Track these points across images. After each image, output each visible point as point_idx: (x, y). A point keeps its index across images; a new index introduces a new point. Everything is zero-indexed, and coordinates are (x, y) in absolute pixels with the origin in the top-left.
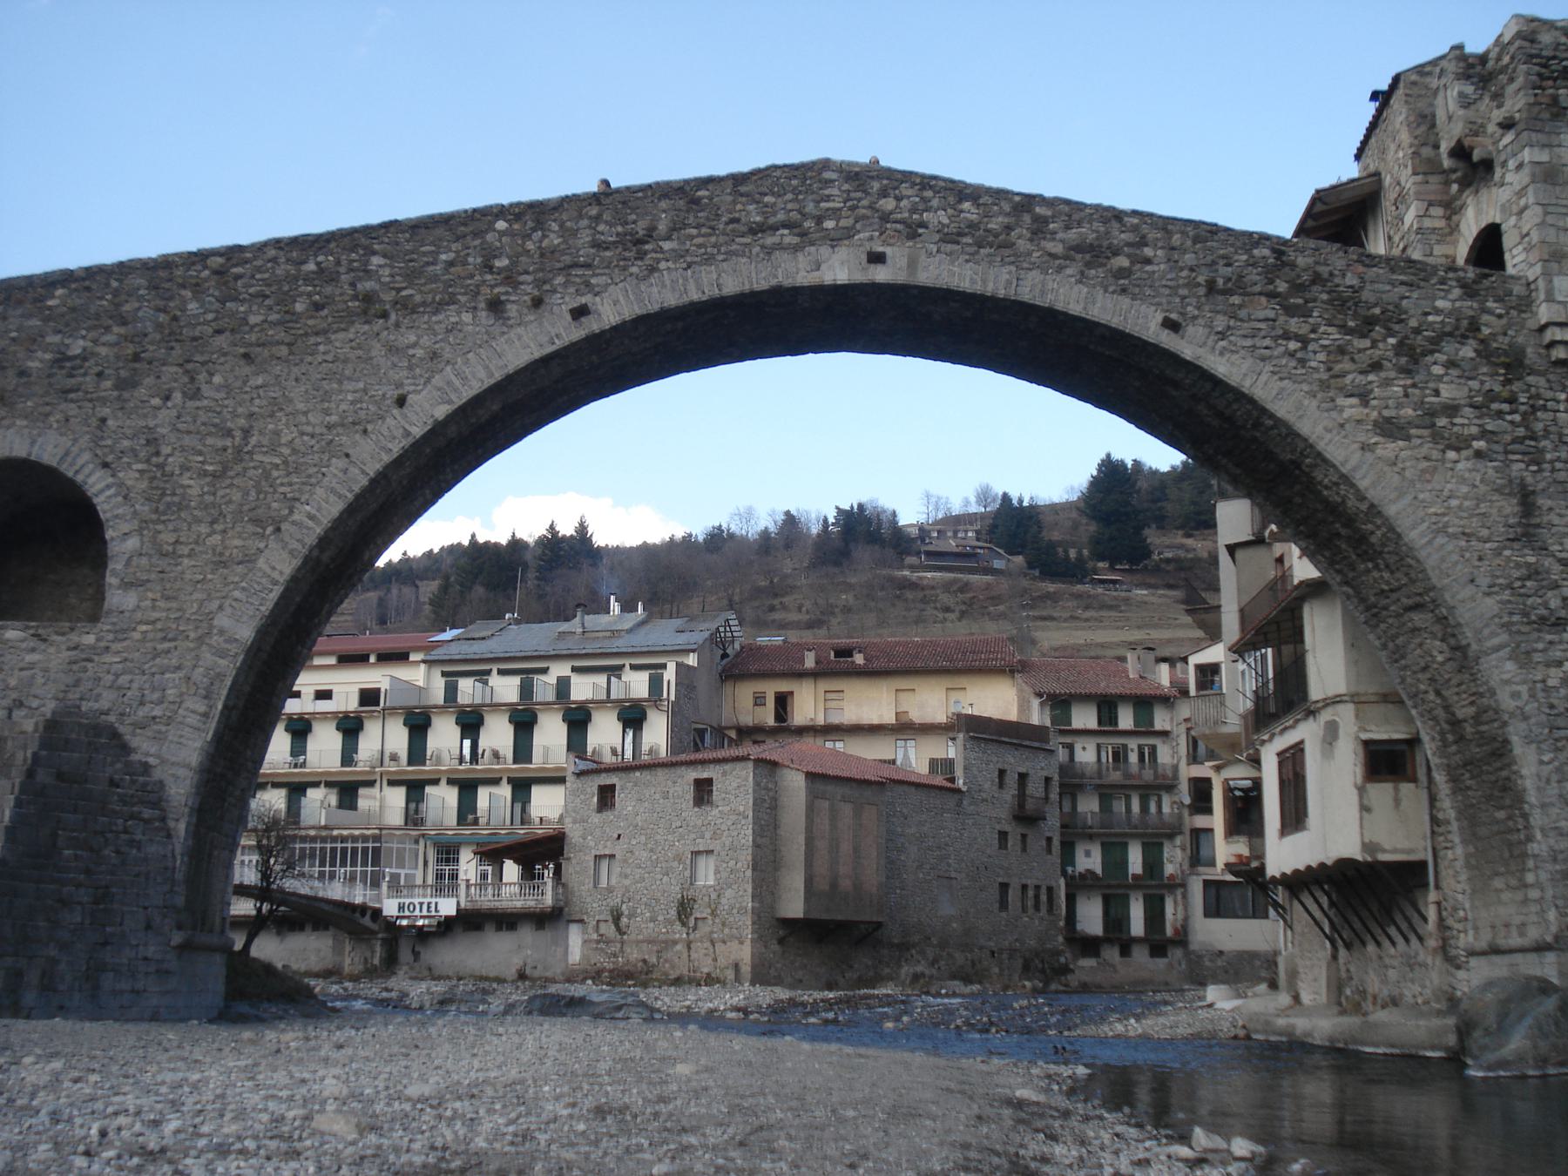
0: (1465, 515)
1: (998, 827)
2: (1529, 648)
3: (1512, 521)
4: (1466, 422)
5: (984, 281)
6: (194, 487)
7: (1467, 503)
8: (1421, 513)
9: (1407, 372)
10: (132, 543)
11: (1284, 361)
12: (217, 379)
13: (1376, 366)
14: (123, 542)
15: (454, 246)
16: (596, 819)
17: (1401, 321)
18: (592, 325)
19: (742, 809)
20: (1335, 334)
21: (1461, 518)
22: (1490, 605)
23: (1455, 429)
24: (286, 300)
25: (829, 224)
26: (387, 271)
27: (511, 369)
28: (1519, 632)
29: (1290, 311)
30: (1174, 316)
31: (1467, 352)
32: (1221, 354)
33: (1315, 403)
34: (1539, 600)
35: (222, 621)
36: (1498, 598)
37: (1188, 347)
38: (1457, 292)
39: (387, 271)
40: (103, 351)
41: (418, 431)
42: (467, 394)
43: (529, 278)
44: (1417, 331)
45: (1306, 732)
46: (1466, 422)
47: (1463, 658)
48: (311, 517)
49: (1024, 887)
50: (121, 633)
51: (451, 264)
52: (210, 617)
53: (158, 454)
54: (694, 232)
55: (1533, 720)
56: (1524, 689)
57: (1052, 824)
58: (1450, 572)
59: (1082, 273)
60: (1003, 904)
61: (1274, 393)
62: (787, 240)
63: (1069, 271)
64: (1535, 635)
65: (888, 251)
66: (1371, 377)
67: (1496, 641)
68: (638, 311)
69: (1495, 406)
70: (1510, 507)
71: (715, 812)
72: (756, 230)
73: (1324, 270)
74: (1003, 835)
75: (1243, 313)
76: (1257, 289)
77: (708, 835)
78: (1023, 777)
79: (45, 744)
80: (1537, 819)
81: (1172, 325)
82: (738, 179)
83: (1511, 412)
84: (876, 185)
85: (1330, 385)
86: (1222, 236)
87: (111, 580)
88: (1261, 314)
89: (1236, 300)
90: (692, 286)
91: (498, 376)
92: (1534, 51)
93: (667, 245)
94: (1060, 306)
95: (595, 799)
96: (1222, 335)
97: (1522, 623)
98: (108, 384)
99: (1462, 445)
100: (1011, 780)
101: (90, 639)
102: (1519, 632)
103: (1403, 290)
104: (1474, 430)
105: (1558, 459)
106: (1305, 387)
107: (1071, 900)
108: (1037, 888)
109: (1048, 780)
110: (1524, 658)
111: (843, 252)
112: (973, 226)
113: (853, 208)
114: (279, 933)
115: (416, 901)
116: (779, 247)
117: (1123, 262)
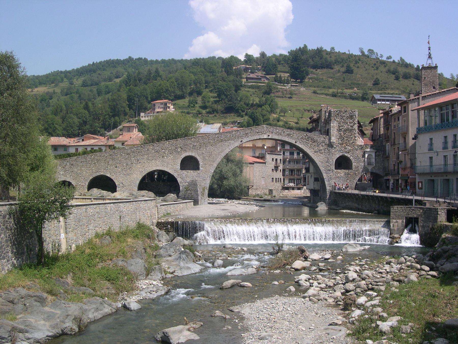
1: (272, 168)
4: (323, 151)
6: (207, 158)
13: (315, 146)
14: (201, 163)
24: (214, 140)
29: (307, 140)
31: (324, 144)
35: (210, 170)
37: (297, 144)
45: (309, 175)
46: (323, 151)
47: (321, 173)
49: (276, 178)
50: (202, 171)
57: (281, 168)
60: (273, 181)
70: (326, 159)
72: (257, 133)
74: (273, 170)
78: (276, 160)
80: (327, 188)
81: (296, 142)
85: (310, 147)
100: (275, 160)
107: (284, 179)
108: (278, 178)
109: (281, 160)
110: (326, 173)
112: (278, 132)
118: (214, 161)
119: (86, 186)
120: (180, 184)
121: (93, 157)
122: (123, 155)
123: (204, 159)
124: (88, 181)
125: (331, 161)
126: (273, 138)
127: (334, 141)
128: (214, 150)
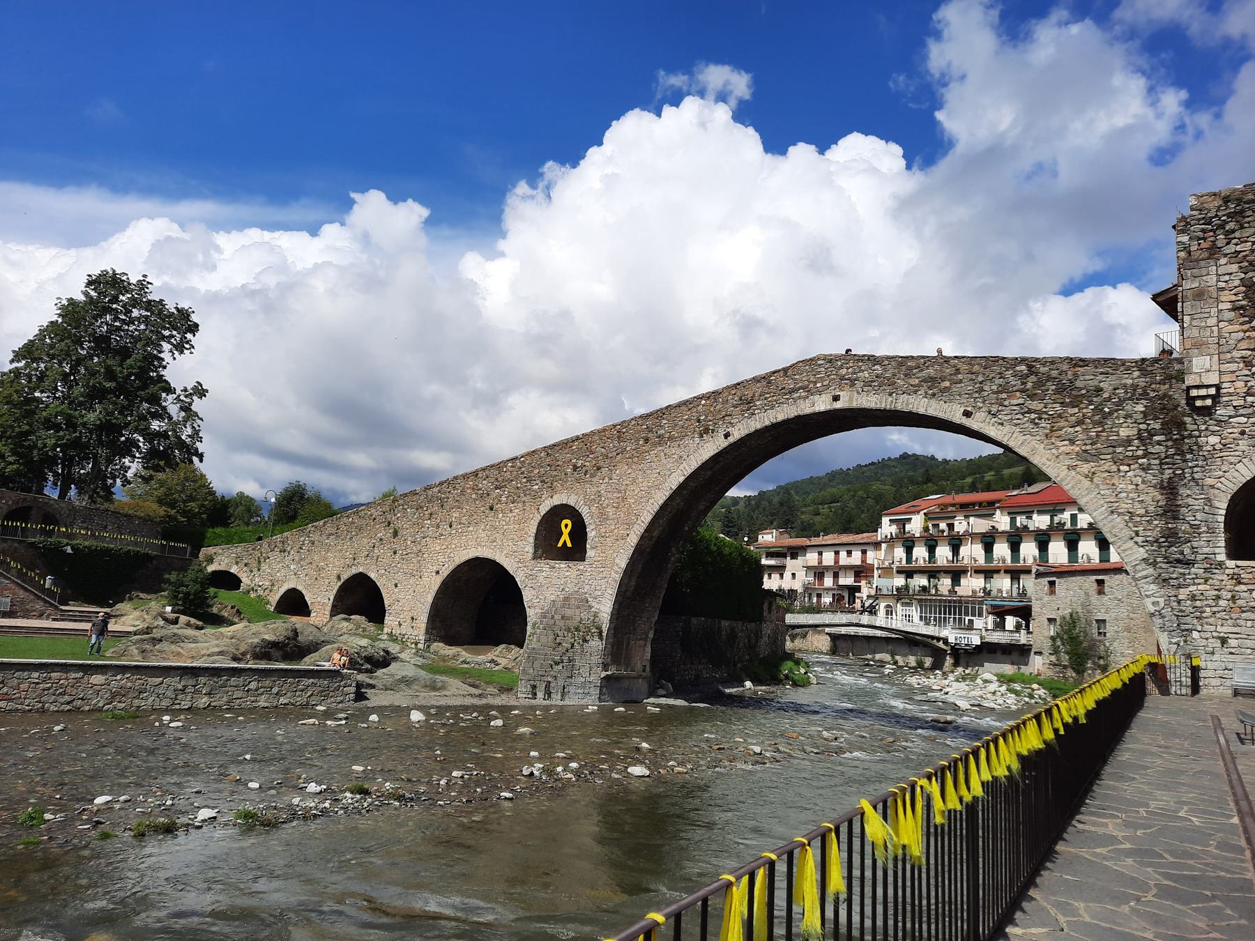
0: (1131, 501)
2: (1167, 577)
3: (1160, 504)
5: (881, 403)
6: (610, 511)
7: (1131, 495)
8: (1102, 502)
9: (1100, 423)
10: (594, 533)
11: (1027, 425)
12: (618, 472)
13: (1080, 423)
15: (689, 413)
16: (1046, 598)
17: (1099, 395)
18: (731, 440)
19: (1120, 597)
20: (1058, 407)
21: (1127, 504)
22: (1142, 553)
23: (1127, 453)
25: (819, 385)
26: (666, 426)
27: (704, 460)
28: (1161, 568)
29: (1032, 397)
30: (969, 409)
32: (993, 425)
33: (1042, 446)
34: (1176, 549)
35: (617, 561)
36: (1147, 548)
38: (1136, 374)
39: (666, 426)
40: (587, 464)
41: (674, 488)
42: (690, 471)
43: (711, 423)
44: (1109, 399)
48: (643, 522)
51: (686, 420)
52: (614, 559)
53: (600, 500)
54: (768, 396)
55: (1166, 619)
56: (1161, 601)
58: (1118, 534)
59: (926, 393)
61: (1019, 443)
62: (803, 394)
63: (919, 393)
64: (1172, 569)
65: (841, 393)
66: (1078, 429)
67: (1144, 573)
68: (747, 432)
69: (1156, 438)
71: (1106, 599)
73: (1054, 373)
75: (1006, 403)
76: (1015, 389)
77: (1103, 611)
79: (563, 607)
81: (967, 414)
82: (785, 370)
83: (1167, 440)
84: (839, 363)
86: (1001, 362)
87: (588, 546)
88: (1015, 402)
89: (1004, 396)
90: (766, 419)
91: (700, 463)
92: (1200, 216)
93: (758, 403)
94: (914, 410)
95: (1046, 588)
96: (994, 415)
97: (1164, 562)
98: (588, 476)
99: (1131, 462)
101: (582, 567)
102: (1161, 568)
103: (1100, 377)
104: (1140, 453)
105: (1197, 466)
106: (1038, 438)
111: (823, 396)
113: (828, 376)
114: (909, 646)
115: (962, 636)
116: (800, 398)
117: (947, 384)
118: (629, 525)
119: (329, 608)
120: (527, 610)
121: (350, 519)
122: (409, 510)
123: (603, 517)
124: (335, 592)
125: (1198, 504)
126: (854, 405)
127: (1213, 379)
128: (634, 480)
